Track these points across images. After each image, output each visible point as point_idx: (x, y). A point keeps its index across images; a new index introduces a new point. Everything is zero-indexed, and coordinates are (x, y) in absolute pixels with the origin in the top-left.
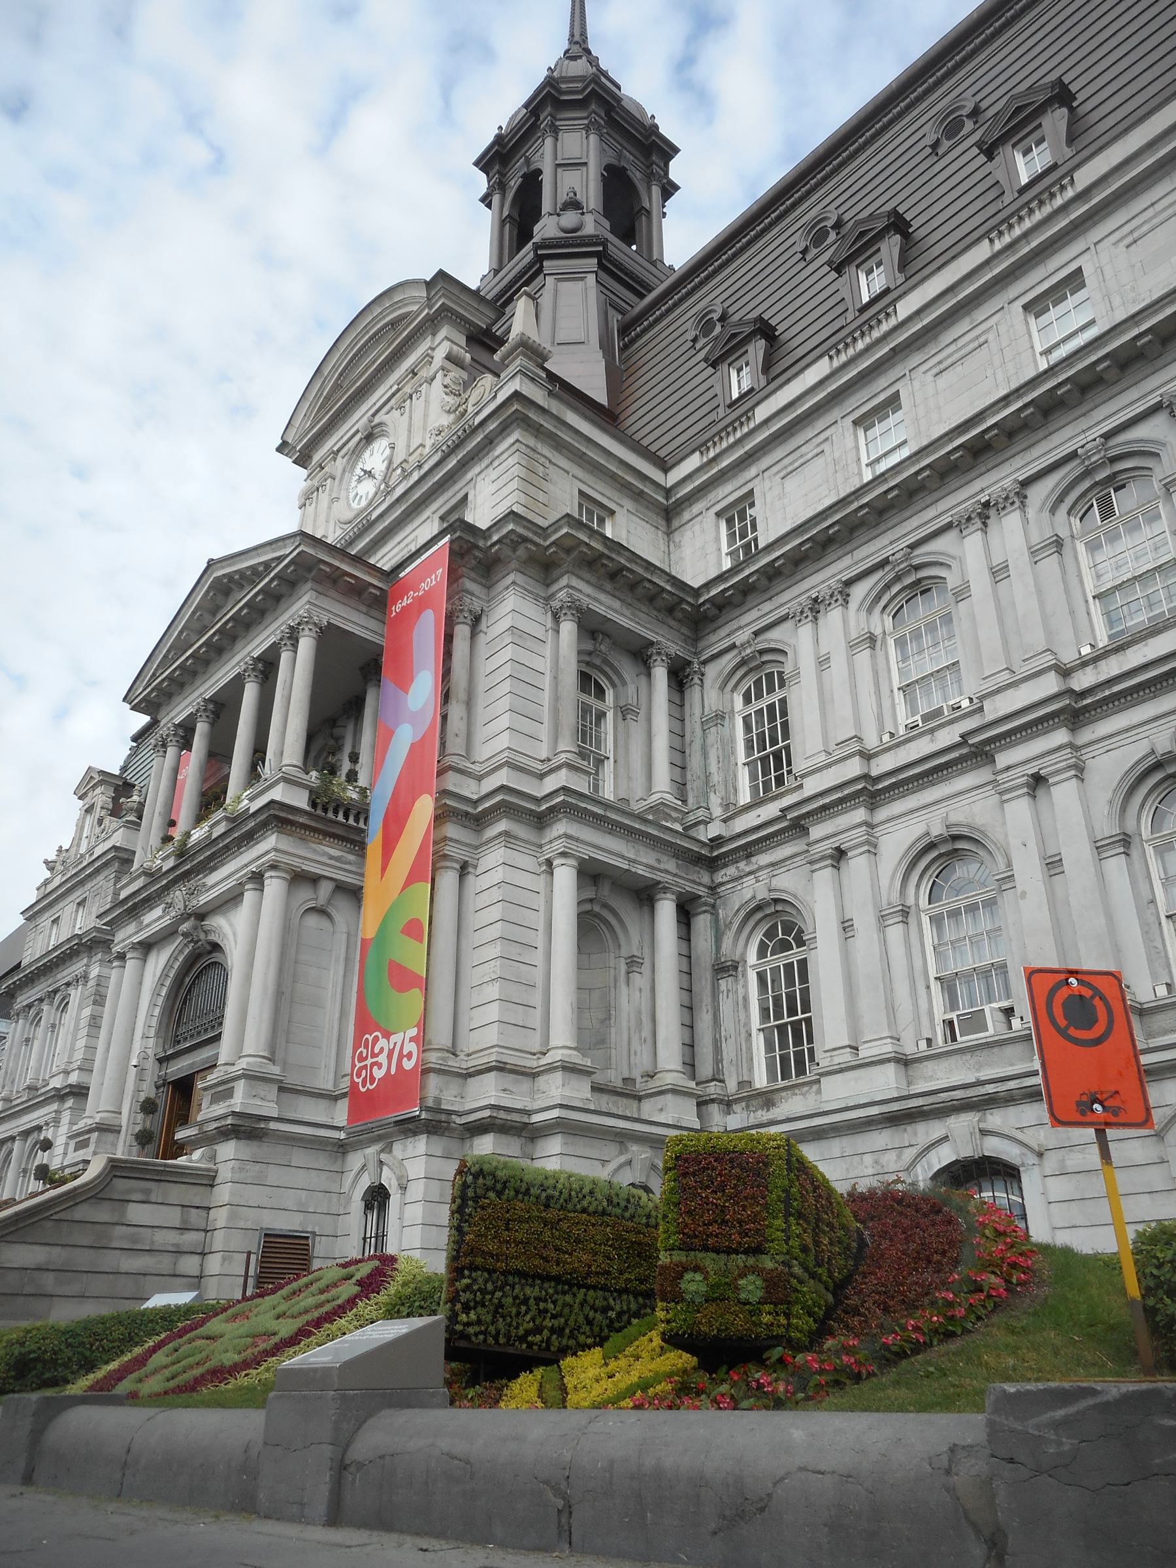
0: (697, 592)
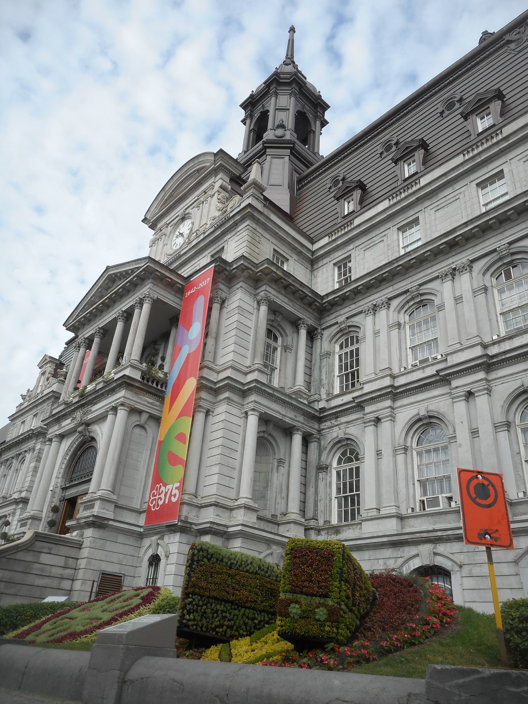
0: (322, 298)
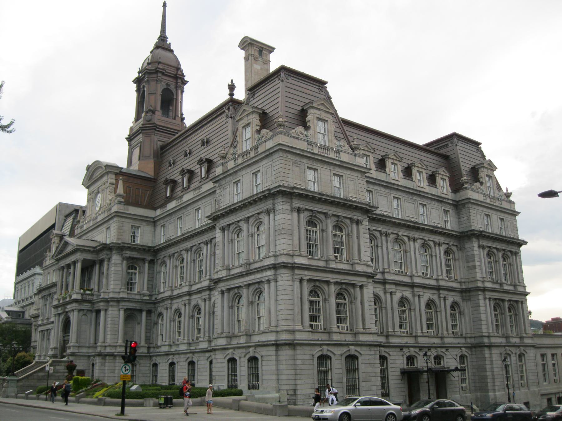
0: (154, 247)
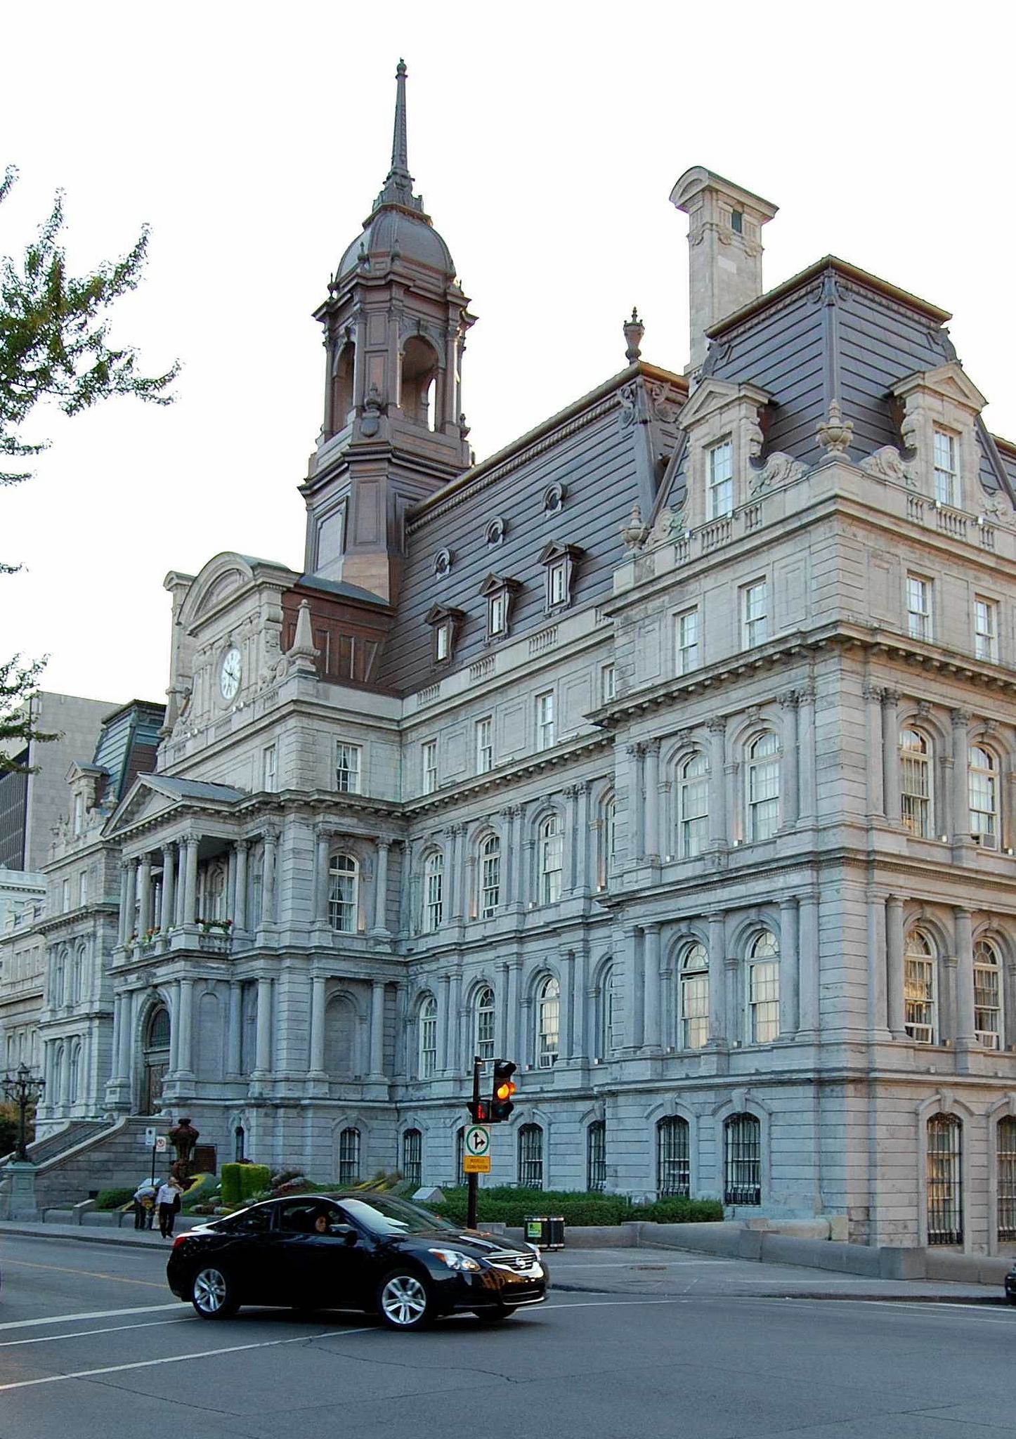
0: (403, 805)
